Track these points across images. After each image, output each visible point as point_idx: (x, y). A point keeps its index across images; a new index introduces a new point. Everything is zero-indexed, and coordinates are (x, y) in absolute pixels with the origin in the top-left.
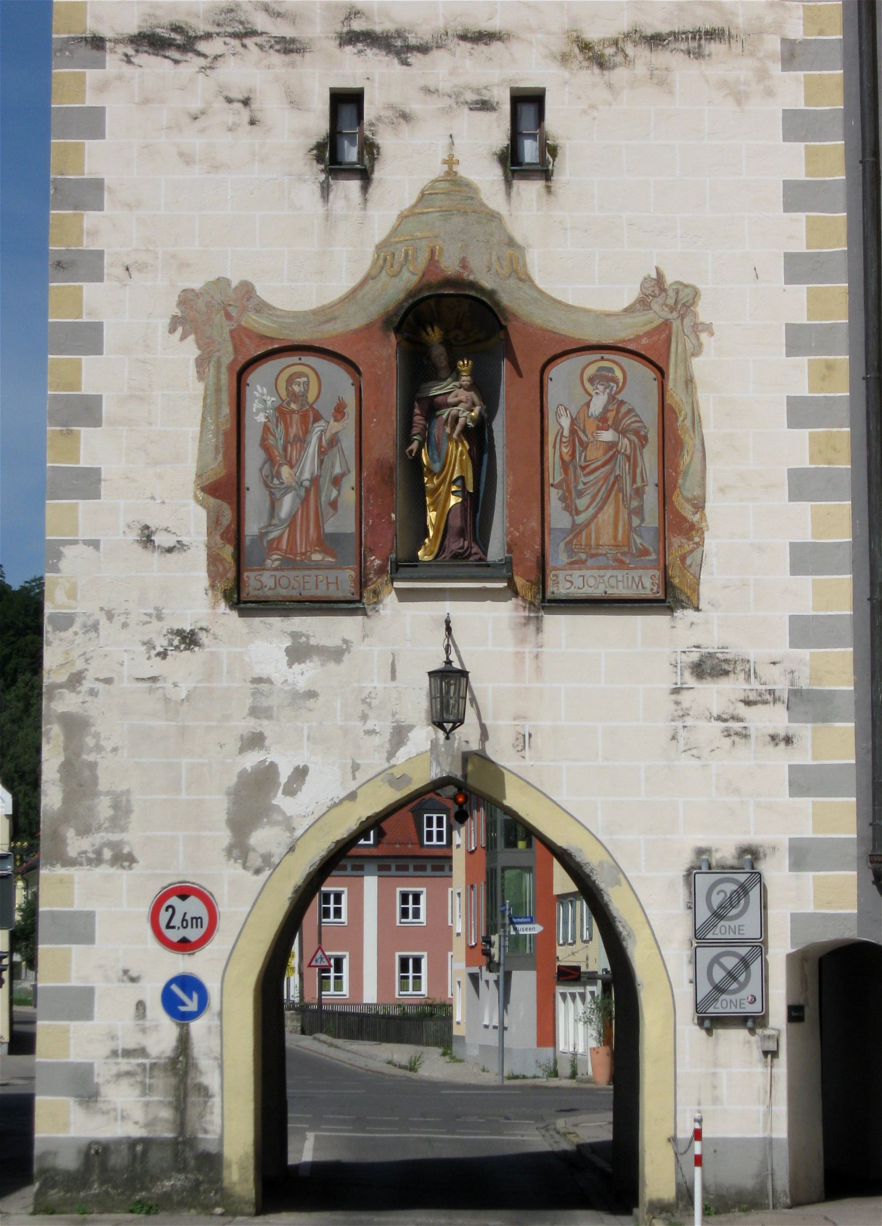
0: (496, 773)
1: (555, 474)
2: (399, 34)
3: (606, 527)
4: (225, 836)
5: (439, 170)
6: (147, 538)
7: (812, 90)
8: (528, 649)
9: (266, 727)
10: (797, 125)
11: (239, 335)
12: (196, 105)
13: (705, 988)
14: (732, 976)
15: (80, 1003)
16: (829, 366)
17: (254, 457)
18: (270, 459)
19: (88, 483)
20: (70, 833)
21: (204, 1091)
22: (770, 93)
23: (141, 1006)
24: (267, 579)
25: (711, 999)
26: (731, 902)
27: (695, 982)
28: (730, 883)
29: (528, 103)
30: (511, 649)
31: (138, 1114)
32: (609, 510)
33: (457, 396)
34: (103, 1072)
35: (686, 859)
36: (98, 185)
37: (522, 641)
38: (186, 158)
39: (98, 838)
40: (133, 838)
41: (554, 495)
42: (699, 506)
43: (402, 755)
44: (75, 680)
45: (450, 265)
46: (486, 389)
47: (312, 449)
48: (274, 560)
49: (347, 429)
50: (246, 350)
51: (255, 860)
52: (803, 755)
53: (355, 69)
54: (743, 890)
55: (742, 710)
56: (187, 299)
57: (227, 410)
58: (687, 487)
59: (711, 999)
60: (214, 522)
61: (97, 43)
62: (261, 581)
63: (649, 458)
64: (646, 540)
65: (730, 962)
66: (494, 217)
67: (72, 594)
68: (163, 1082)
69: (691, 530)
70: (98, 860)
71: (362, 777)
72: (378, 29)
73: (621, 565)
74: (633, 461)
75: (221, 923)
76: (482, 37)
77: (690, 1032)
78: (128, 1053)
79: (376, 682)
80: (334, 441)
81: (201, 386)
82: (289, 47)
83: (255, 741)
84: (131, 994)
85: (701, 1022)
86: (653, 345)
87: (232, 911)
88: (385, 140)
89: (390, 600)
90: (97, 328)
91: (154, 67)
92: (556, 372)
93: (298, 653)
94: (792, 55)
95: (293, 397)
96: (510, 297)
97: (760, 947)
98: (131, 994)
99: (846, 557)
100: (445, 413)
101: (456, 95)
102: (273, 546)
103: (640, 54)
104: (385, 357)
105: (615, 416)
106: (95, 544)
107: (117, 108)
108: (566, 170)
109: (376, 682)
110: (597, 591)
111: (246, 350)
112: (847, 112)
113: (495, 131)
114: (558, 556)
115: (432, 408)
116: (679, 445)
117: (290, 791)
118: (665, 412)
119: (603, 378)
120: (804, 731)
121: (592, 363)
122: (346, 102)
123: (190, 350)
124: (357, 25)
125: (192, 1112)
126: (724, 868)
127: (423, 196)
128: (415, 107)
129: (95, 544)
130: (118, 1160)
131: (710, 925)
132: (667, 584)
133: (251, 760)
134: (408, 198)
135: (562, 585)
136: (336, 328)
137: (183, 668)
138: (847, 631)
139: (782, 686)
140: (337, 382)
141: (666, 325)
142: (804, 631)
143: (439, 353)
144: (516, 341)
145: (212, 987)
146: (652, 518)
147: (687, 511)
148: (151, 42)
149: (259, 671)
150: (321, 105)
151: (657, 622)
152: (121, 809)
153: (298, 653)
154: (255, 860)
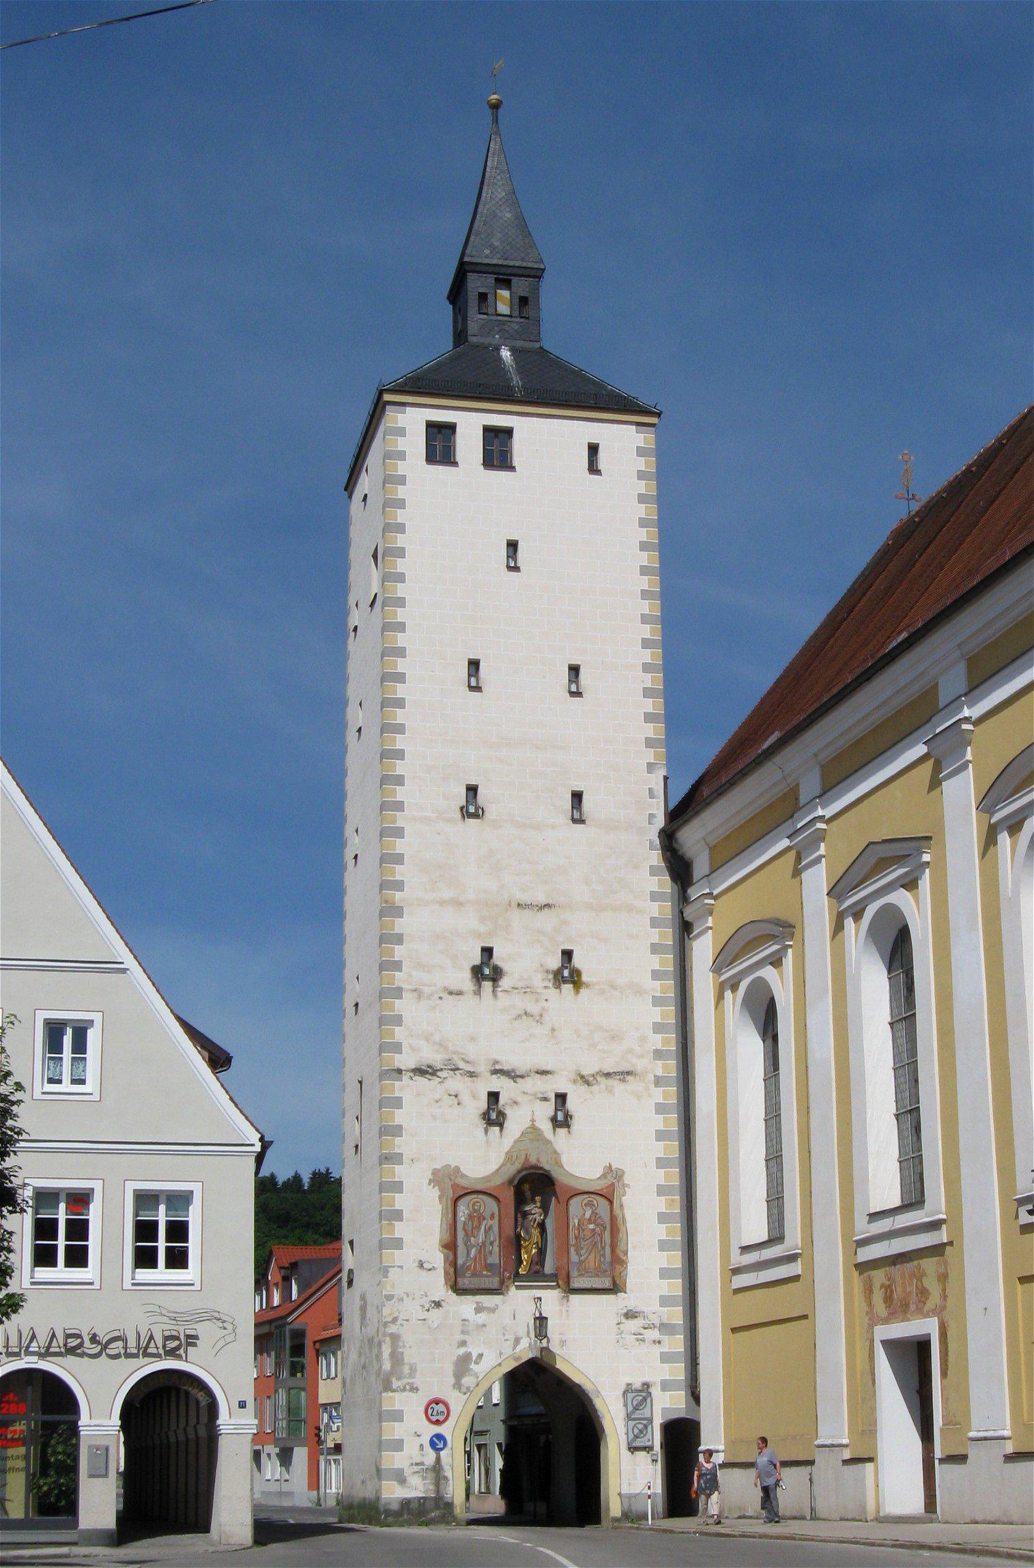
0: (553, 1355)
1: (572, 1241)
2: (513, 1071)
3: (591, 1262)
4: (452, 1380)
5: (529, 1124)
6: (421, 1265)
7: (665, 1094)
8: (564, 1308)
9: (466, 1337)
10: (660, 1109)
11: (455, 1186)
12: (438, 1097)
13: (631, 1436)
14: (641, 1432)
15: (398, 1445)
16: (673, 1201)
17: (460, 1234)
18: (467, 1235)
19: (398, 1244)
20: (394, 1380)
21: (446, 1478)
22: (650, 1096)
23: (421, 1446)
24: (466, 1281)
26: (640, 1404)
27: (627, 1434)
28: (639, 1396)
29: (561, 1098)
30: (558, 1308)
31: (421, 1488)
32: (593, 1255)
33: (534, 1209)
34: (407, 1472)
35: (623, 1388)
36: (400, 1127)
37: (562, 1305)
38: (434, 1118)
39: (405, 1381)
40: (417, 1381)
41: (572, 1249)
42: (626, 1253)
43: (519, 1348)
44: (395, 1320)
45: (533, 1160)
46: (545, 1208)
48: (468, 1274)
49: (495, 1223)
50: (458, 1193)
52: (665, 1348)
53: (497, 1084)
54: (645, 1399)
55: (642, 1331)
57: (450, 1216)
58: (621, 1246)
60: (446, 1259)
61: (399, 1071)
62: (464, 1282)
63: (607, 1234)
64: (605, 1266)
65: (640, 1426)
66: (549, 1142)
68: (431, 1475)
69: (623, 1263)
70: (404, 1390)
71: (503, 1357)
73: (597, 1276)
74: (601, 1236)
77: (625, 1453)
78: (417, 1464)
79: (508, 1321)
80: (490, 1228)
81: (440, 1207)
82: (472, 1075)
83: (463, 1343)
84: (418, 1441)
85: (629, 1449)
86: (608, 1192)
87: (455, 1409)
88: (509, 1112)
89: (513, 1289)
92: (572, 1202)
93: (479, 1309)
94: (658, 1081)
95: (475, 1211)
96: (556, 1174)
97: (651, 1420)
98: (418, 1441)
99: (680, 1273)
100: (531, 1217)
101: (534, 1095)
102: (468, 1268)
104: (509, 1196)
105: (594, 1218)
106: (401, 1267)
107: (407, 1098)
108: (576, 1124)
109: (508, 1321)
110: (589, 1286)
111: (458, 1193)
112: (678, 1104)
113: (549, 1108)
114: (574, 1273)
115: (525, 1215)
116: (618, 1231)
118: (613, 1218)
119: (590, 1204)
120: (665, 1338)
122: (494, 1097)
123: (436, 1192)
124: (498, 1067)
125: (442, 1487)
128: (519, 1099)
129: (401, 1267)
130: (414, 1505)
131: (633, 1413)
132: (614, 1283)
133: (462, 1351)
134: (517, 1135)
135: (577, 1283)
136: (492, 1184)
137: (436, 1314)
138: (680, 1300)
139: (657, 1322)
140: (492, 1205)
141: (613, 1184)
142: (665, 1301)
144: (558, 1190)
145: (449, 1438)
147: (621, 1255)
148: (420, 1071)
150: (485, 1098)
151: (612, 1297)
152: (413, 1370)
153: (479, 1309)
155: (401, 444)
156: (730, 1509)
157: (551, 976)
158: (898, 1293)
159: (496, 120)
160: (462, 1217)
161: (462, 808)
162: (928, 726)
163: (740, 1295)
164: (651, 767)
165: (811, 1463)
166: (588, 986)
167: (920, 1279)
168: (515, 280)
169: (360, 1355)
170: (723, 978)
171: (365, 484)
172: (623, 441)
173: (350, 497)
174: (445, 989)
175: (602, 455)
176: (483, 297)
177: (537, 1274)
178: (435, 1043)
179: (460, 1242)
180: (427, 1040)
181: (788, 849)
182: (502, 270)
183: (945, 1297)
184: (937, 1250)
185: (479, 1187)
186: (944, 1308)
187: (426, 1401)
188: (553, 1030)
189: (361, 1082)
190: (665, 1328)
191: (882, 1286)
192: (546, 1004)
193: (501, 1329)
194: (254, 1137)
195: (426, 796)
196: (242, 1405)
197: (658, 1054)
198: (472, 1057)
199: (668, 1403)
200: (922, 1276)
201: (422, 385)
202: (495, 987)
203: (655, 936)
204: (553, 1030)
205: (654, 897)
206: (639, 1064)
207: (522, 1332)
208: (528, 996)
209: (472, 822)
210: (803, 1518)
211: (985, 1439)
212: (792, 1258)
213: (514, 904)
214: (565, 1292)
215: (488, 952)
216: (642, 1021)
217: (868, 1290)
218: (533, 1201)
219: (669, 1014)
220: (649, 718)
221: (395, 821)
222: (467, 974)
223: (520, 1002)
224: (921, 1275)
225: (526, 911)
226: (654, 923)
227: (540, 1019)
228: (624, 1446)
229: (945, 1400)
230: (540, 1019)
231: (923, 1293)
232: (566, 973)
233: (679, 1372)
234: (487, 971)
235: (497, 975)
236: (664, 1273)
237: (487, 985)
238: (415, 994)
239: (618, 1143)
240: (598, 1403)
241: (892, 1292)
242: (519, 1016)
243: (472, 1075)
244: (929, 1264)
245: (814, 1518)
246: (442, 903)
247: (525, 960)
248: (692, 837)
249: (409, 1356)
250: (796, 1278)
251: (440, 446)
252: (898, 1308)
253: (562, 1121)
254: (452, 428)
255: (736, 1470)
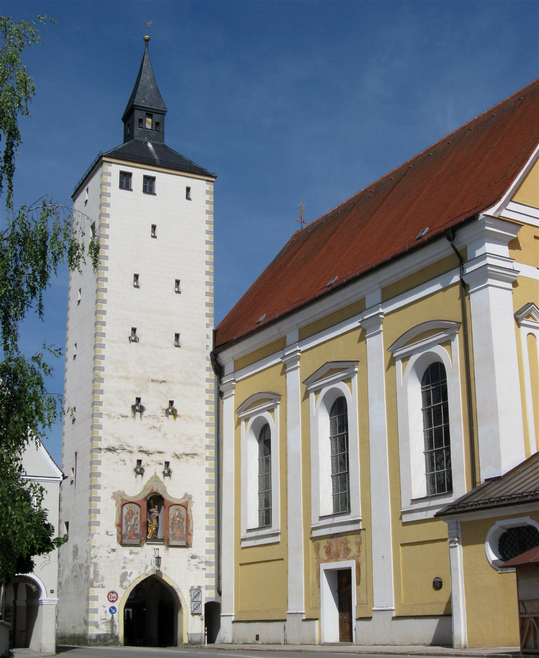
0: (161, 573)
1: (170, 525)
2: (148, 451)
3: (178, 534)
4: (119, 583)
6: (107, 533)
7: (210, 464)
8: (166, 554)
9: (126, 565)
10: (208, 470)
11: (122, 500)
13: (193, 609)
14: (197, 607)
15: (96, 611)
16: (212, 509)
17: (124, 520)
18: (127, 521)
19: (98, 524)
20: (95, 582)
21: (116, 626)
22: (204, 464)
23: (106, 611)
24: (126, 541)
25: (194, 610)
26: (197, 595)
27: (191, 608)
28: (196, 592)
29: (167, 464)
31: (105, 629)
32: (178, 532)
35: (190, 588)
36: (100, 473)
39: (99, 583)
40: (104, 583)
41: (170, 528)
42: (192, 531)
43: (147, 570)
44: (96, 557)
45: (155, 490)
46: (159, 510)
47: (133, 519)
50: (124, 502)
51: (124, 587)
53: (141, 456)
54: (199, 593)
55: (198, 564)
56: (114, 493)
57: (120, 512)
58: (190, 528)
59: (194, 610)
60: (118, 531)
61: (100, 449)
62: (125, 541)
65: (197, 605)
66: (162, 482)
67: (95, 542)
68: (109, 624)
69: (191, 535)
70: (99, 587)
72: (145, 450)
73: (180, 540)
75: (119, 598)
76: (160, 453)
77: (190, 616)
78: (104, 619)
80: (136, 518)
81: (116, 509)
82: (131, 452)
84: (105, 609)
85: (192, 614)
88: (145, 468)
89: (145, 544)
90: (100, 497)
91: (109, 453)
92: (171, 508)
93: (131, 553)
94: (207, 458)
95: (131, 511)
96: (164, 496)
97: (201, 602)
98: (105, 609)
101: (156, 462)
103: (184, 456)
104: (144, 505)
105: (180, 516)
106: (99, 534)
108: (173, 475)
111: (124, 502)
113: (162, 468)
114: (171, 539)
115: (151, 513)
116: (189, 521)
117: (130, 576)
118: (187, 516)
119: (178, 509)
120: (207, 567)
121: (176, 507)
122: (139, 462)
124: (141, 449)
125: (114, 629)
126: (195, 589)
127: (151, 478)
128: (150, 463)
129: (99, 534)
130: (102, 637)
131: (194, 599)
132: (187, 543)
133: (123, 571)
135: (172, 543)
140: (137, 508)
141: (187, 502)
142: (208, 552)
143: (152, 504)
146: (185, 533)
147: (190, 532)
148: (109, 450)
149: (125, 556)
150: (136, 462)
151: (186, 549)
152: (103, 578)
153: (131, 553)
154: (124, 587)
155: (109, 179)
156: (238, 640)
157: (165, 412)
158: (334, 550)
159: (147, 46)
160: (125, 513)
161: (130, 338)
162: (360, 315)
163: (245, 550)
164: (208, 326)
165: (285, 620)
166: (179, 416)
167: (346, 544)
168: (154, 115)
169: (73, 571)
170: (241, 416)
171: (84, 195)
172: (201, 187)
173: (74, 200)
174: (121, 415)
175: (192, 192)
176: (141, 121)
177: (155, 539)
178: (115, 438)
179: (124, 524)
180: (112, 436)
181: (280, 363)
182: (150, 110)
183: (360, 552)
184: (357, 532)
185: (132, 500)
186: (358, 556)
187: (108, 592)
188: (165, 434)
189: (76, 454)
190: (208, 563)
191: (325, 547)
192: (162, 423)
193: (139, 562)
194: (60, 474)
195: (114, 332)
196: (52, 592)
197: (208, 447)
198: (131, 445)
199: (208, 595)
200: (347, 543)
201: (118, 155)
202: (141, 415)
203: (207, 397)
204: (165, 434)
205: (208, 380)
206: (200, 451)
207: (149, 563)
208: (155, 419)
209: (133, 344)
210: (280, 644)
211: (382, 610)
212: (276, 535)
213: (150, 380)
214: (167, 546)
215: (138, 400)
216: (201, 432)
217: (317, 549)
218: (155, 508)
219: (212, 430)
220: (207, 304)
221: (101, 341)
222: (130, 409)
223: (151, 422)
224: (347, 542)
225: (155, 383)
226: (207, 391)
227: (159, 430)
228: (190, 612)
229: (358, 595)
230: (159, 430)
231: (348, 550)
232: (170, 411)
233: (212, 582)
234: (138, 408)
235: (142, 410)
236: (208, 540)
237: (138, 414)
238: (108, 416)
239: (189, 484)
240: (179, 595)
241: (330, 549)
242: (151, 428)
243: (131, 452)
244: (352, 539)
245: (286, 643)
246: (120, 377)
247: (154, 404)
248: (227, 357)
249: (101, 572)
250: (278, 543)
251: (125, 181)
252: (331, 555)
253: (168, 473)
254: (130, 175)
255: (242, 624)
